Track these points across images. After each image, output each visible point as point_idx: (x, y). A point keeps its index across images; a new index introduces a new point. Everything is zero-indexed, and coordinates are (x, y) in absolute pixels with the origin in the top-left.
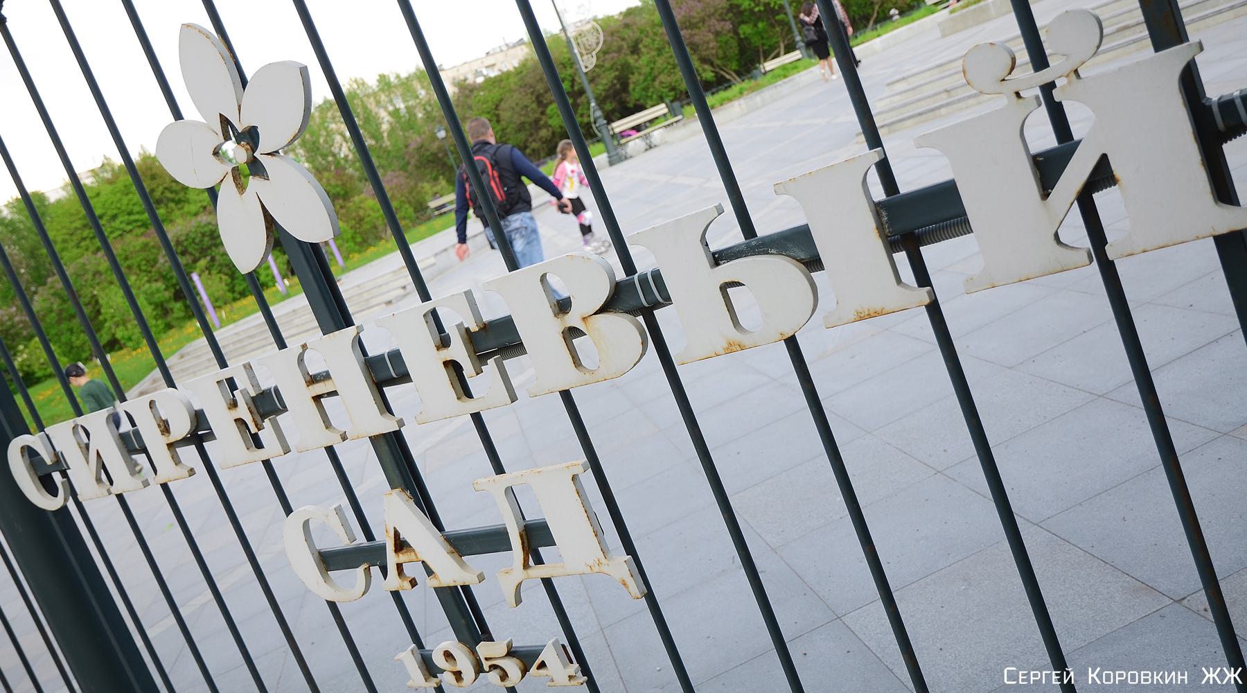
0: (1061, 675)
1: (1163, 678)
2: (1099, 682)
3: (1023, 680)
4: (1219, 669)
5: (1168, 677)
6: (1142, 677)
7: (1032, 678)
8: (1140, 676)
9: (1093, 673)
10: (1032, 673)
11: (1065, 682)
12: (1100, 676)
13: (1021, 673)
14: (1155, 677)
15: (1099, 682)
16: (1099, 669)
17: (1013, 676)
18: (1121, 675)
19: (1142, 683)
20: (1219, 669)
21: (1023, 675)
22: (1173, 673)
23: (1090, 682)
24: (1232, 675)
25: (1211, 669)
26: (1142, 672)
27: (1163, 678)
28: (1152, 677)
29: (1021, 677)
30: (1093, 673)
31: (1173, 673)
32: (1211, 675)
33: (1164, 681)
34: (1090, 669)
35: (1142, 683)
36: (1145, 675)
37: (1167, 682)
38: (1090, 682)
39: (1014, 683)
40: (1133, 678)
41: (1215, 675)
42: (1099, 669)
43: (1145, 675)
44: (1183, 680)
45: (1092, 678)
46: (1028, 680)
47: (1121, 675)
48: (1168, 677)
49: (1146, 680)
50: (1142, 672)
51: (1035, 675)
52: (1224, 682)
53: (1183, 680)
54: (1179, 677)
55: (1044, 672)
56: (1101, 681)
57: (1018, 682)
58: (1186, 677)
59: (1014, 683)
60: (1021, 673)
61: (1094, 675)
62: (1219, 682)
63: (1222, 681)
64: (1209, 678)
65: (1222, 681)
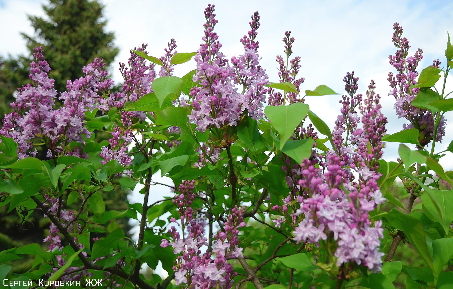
0: (27, 282)
1: (69, 283)
2: (43, 285)
3: (11, 285)
4: (93, 280)
6: (61, 283)
8: (60, 284)
9: (40, 282)
10: (15, 281)
11: (29, 285)
13: (10, 281)
14: (66, 283)
17: (7, 283)
19: (61, 286)
20: (93, 280)
21: (11, 282)
22: (74, 282)
24: (98, 283)
26: (61, 281)
28: (65, 283)
29: (10, 283)
30: (40, 282)
32: (90, 283)
33: (70, 285)
34: (39, 280)
35: (61, 286)
36: (62, 282)
37: (71, 285)
39: (8, 286)
40: (57, 284)
41: (91, 283)
43: (62, 282)
44: (78, 285)
46: (13, 284)
49: (62, 284)
50: (61, 281)
51: (16, 282)
52: (95, 285)
53: (78, 285)
54: (76, 283)
55: (20, 281)
56: (43, 284)
57: (9, 284)
58: (79, 283)
59: (8, 286)
60: (10, 281)
62: (93, 285)
63: (94, 285)
65: (94, 285)
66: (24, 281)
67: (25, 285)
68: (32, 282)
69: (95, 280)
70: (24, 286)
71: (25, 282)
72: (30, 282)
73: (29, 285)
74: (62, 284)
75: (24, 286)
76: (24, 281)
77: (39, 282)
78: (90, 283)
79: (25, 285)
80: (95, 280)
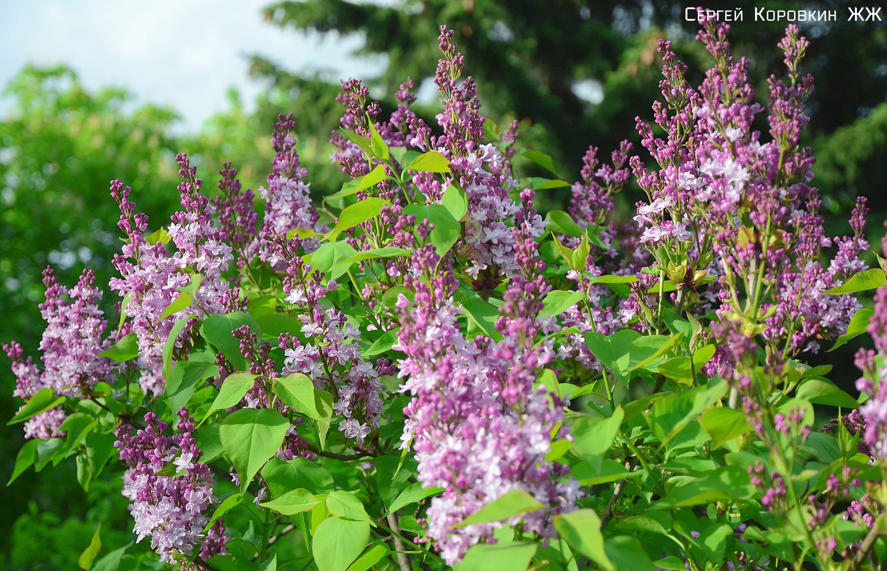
0: (732, 13)
1: (816, 15)
2: (763, 20)
4: (862, 8)
5: (821, 14)
6: (799, 15)
7: (708, 16)
9: (758, 12)
11: (736, 19)
12: (764, 14)
14: (810, 16)
15: (763, 20)
16: (763, 8)
18: (781, 14)
19: (799, 20)
20: (862, 8)
22: (825, 12)
23: (756, 20)
24: (873, 14)
25: (856, 9)
26: (799, 11)
27: (816, 15)
28: (807, 17)
29: (699, 16)
30: (758, 12)
31: (825, 12)
32: (856, 14)
34: (756, 9)
35: (799, 20)
36: (801, 13)
37: (819, 19)
38: (756, 20)
39: (694, 20)
40: (791, 16)
42: (763, 8)
44: (832, 18)
45: (758, 16)
47: (781, 14)
48: (821, 14)
49: (801, 18)
50: (799, 11)
53: (832, 18)
54: (830, 15)
56: (765, 17)
57: (697, 18)
58: (835, 15)
59: (694, 20)
61: (760, 14)
62: (863, 20)
64: (854, 16)
66: (726, 11)
67: (728, 18)
68: (741, 12)
69: (867, 8)
70: (726, 20)
71: (728, 13)
72: (738, 12)
73: (736, 19)
74: (801, 18)
75: (726, 20)
76: (726, 11)
77: (756, 14)
78: (856, 14)
79: (728, 18)
80: (867, 8)
